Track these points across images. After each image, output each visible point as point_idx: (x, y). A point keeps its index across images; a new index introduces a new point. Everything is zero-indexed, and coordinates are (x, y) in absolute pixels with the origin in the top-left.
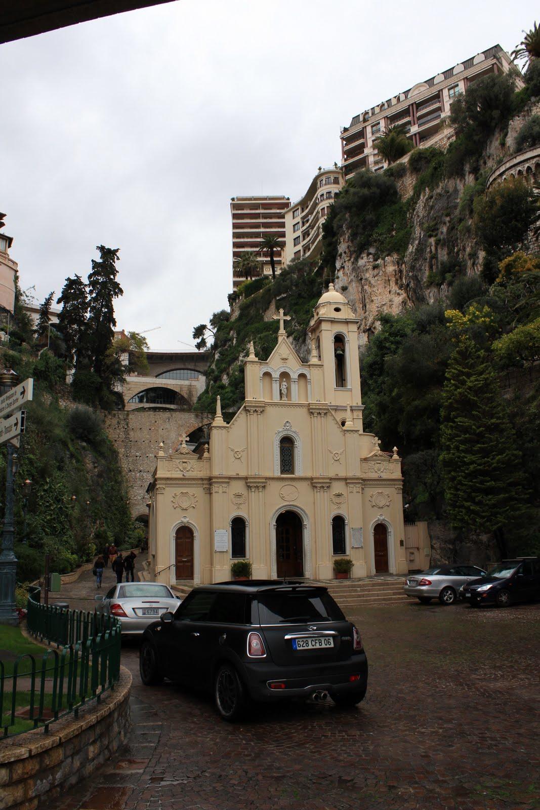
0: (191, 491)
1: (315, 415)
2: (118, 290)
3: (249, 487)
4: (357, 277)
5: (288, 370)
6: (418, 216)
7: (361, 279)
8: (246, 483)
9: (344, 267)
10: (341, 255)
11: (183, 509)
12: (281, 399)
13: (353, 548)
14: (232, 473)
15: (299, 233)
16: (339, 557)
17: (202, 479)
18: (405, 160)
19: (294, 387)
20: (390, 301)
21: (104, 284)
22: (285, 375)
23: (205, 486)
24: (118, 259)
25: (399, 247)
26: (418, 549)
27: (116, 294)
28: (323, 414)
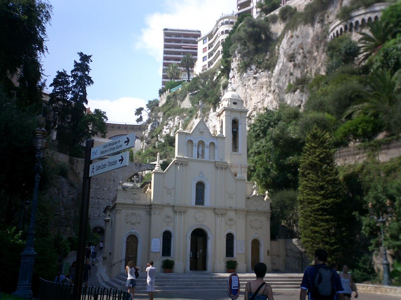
0: (138, 212)
1: (219, 168)
2: (90, 81)
3: (175, 212)
4: (243, 84)
5: (203, 140)
6: (283, 48)
7: (245, 85)
8: (174, 209)
9: (234, 77)
10: (233, 69)
11: (132, 224)
12: (198, 158)
13: (238, 254)
14: (165, 203)
15: (206, 54)
16: (230, 259)
17: (145, 205)
18: (277, 12)
19: (207, 151)
20: (263, 100)
21: (81, 77)
22: (201, 143)
23: (147, 210)
24: (91, 61)
25: (270, 67)
26: (278, 256)
27: (89, 84)
28: (224, 168)
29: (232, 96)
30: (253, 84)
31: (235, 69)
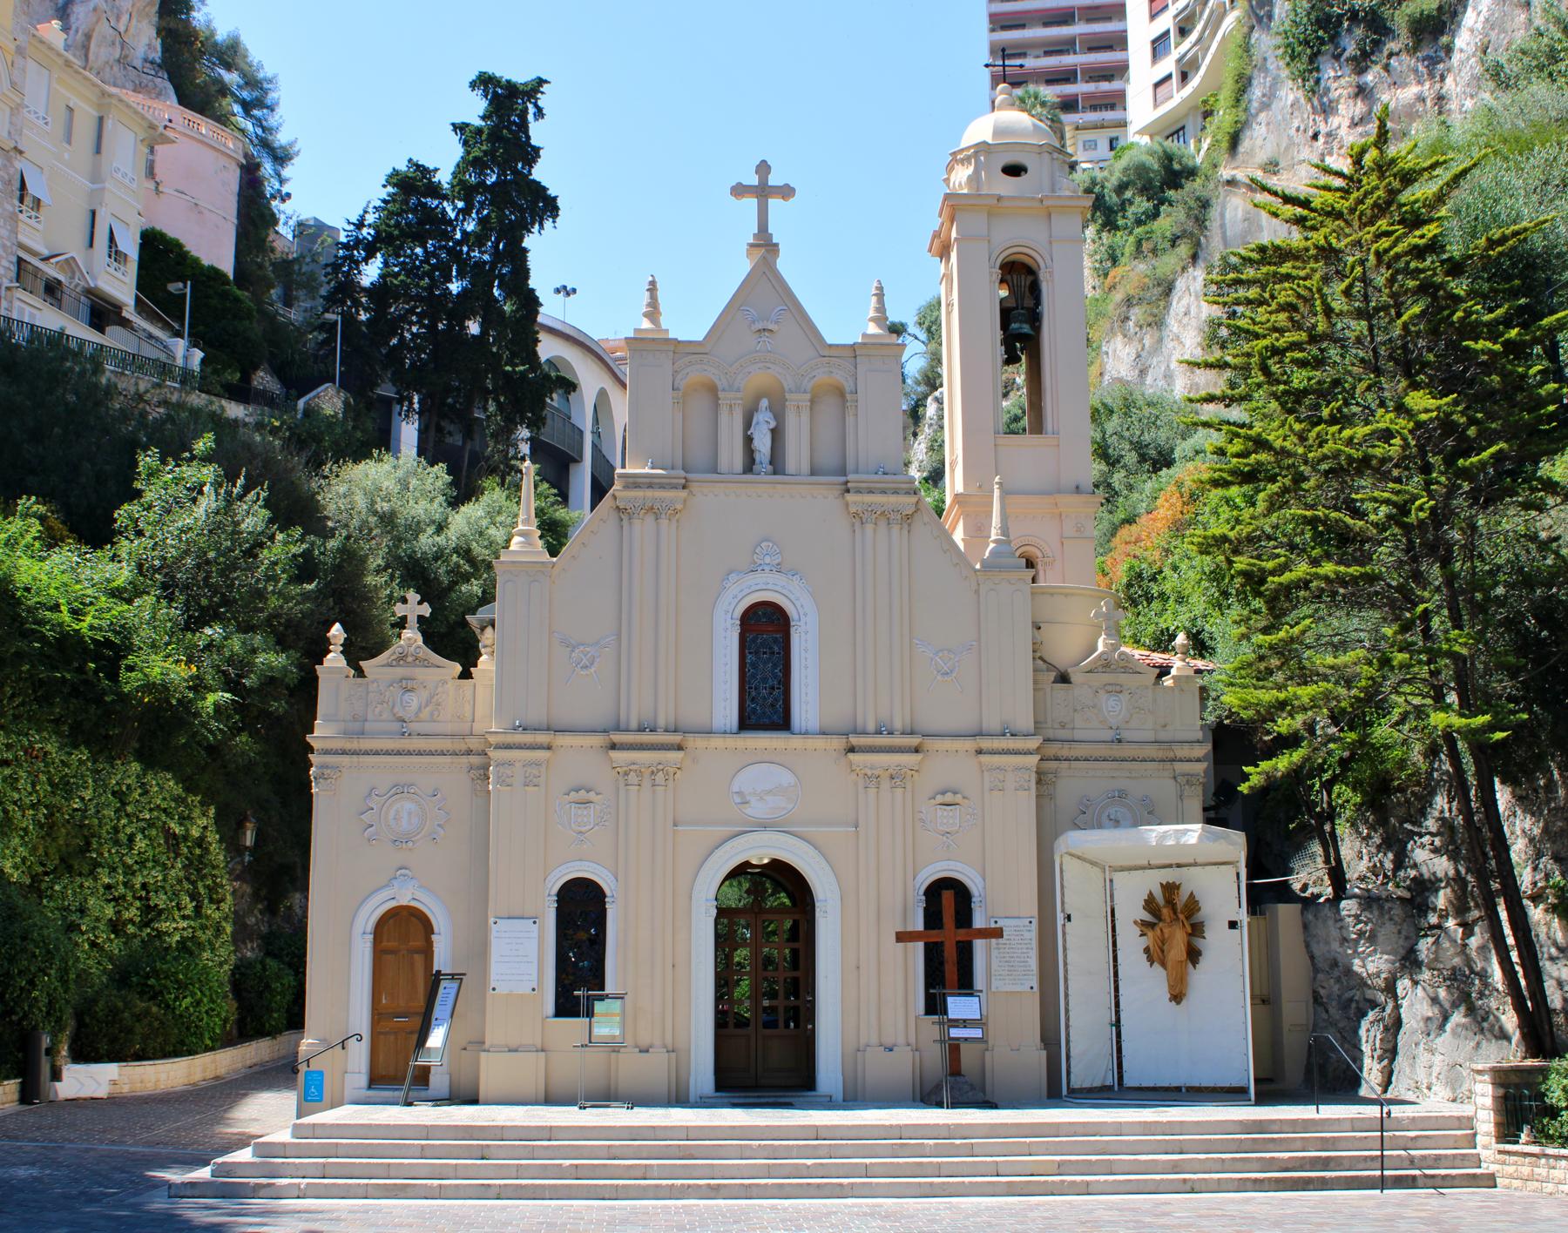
2: (543, 205)
21: (498, 195)
24: (540, 113)
29: (997, 132)
30: (1354, 124)
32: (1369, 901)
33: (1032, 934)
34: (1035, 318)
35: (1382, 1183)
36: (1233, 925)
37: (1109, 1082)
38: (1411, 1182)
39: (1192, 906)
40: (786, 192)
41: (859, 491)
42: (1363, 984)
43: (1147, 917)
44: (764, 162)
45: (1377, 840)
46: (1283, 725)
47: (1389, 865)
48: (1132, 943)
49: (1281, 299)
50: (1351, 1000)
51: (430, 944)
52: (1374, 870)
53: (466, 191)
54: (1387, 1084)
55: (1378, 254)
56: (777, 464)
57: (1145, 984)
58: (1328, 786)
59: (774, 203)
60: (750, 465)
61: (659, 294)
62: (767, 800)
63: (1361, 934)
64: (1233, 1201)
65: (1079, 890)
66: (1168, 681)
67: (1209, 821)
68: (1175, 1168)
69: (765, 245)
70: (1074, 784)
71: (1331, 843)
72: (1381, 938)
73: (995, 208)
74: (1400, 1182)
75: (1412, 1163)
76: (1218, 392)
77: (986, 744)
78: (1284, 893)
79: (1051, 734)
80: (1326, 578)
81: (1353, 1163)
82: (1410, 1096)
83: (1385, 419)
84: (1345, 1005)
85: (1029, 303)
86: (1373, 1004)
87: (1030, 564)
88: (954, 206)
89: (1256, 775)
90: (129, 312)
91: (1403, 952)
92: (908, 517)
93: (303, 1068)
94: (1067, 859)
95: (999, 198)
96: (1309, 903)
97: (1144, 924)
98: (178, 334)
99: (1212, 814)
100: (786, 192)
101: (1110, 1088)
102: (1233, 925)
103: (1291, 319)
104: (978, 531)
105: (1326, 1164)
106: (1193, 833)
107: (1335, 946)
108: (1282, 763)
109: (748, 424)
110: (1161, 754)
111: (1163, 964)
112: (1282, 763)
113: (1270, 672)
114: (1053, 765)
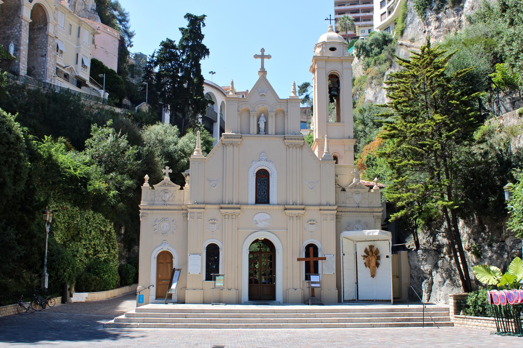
24: (204, 25)
29: (328, 39)
30: (436, 29)
31: (413, 11)
32: (425, 250)
33: (334, 259)
34: (338, 90)
35: (423, 325)
36: (387, 257)
37: (355, 298)
38: (431, 325)
39: (377, 252)
40: (269, 57)
41: (288, 139)
42: (423, 272)
43: (365, 254)
44: (263, 49)
45: (429, 234)
46: (399, 204)
47: (431, 241)
48: (361, 261)
49: (401, 89)
50: (420, 277)
51: (172, 261)
52: (427, 242)
53: (183, 47)
54: (429, 299)
55: (427, 77)
56: (266, 132)
57: (364, 272)
58: (416, 219)
59: (266, 60)
60: (259, 132)
61: (234, 85)
62: (263, 223)
63: (423, 259)
64: (383, 330)
65: (347, 247)
66: (372, 191)
67: (383, 229)
68: (369, 321)
69: (263, 72)
70: (346, 218)
71: (416, 235)
72: (428, 260)
73: (327, 60)
74: (428, 325)
75: (432, 320)
76: (385, 114)
77: (322, 208)
78: (404, 248)
79: (340, 205)
80: (411, 165)
81: (416, 320)
82: (435, 303)
83: (428, 122)
84: (418, 278)
85: (336, 86)
86: (426, 278)
87: (335, 158)
88: (316, 59)
89: (393, 217)
90: (88, 83)
91: (434, 264)
92: (302, 146)
93: (138, 294)
94: (344, 239)
95: (328, 57)
96: (410, 251)
97: (364, 256)
98: (102, 89)
99: (384, 227)
100: (269, 57)
101: (355, 300)
102: (387, 257)
103: (404, 94)
104: (321, 149)
105: (409, 320)
106: (376, 232)
107: (416, 262)
108: (399, 214)
109: (258, 121)
110: (370, 211)
111: (369, 267)
112: (399, 214)
113: (398, 189)
114: (341, 213)
